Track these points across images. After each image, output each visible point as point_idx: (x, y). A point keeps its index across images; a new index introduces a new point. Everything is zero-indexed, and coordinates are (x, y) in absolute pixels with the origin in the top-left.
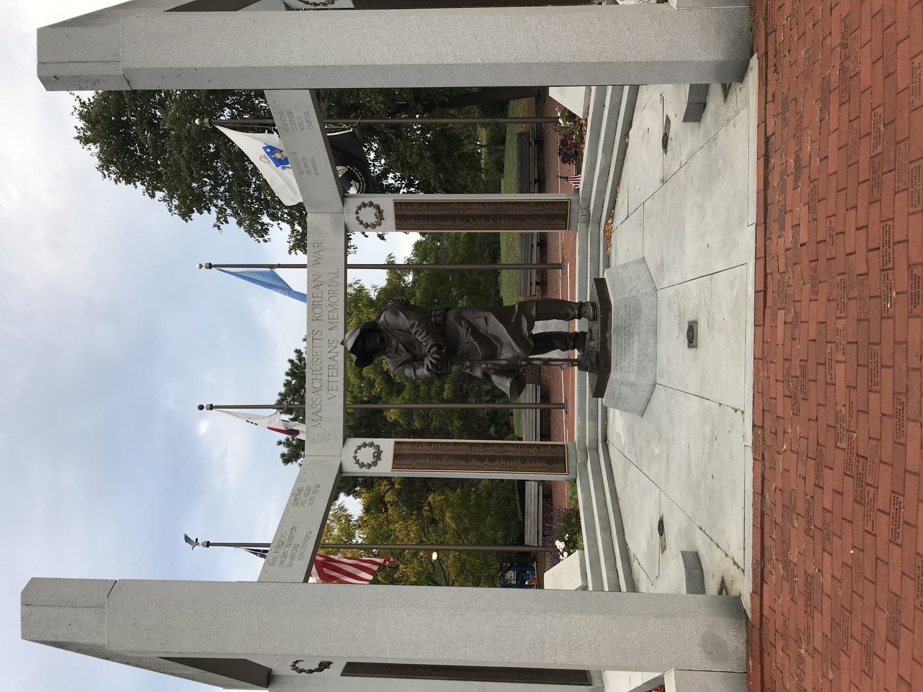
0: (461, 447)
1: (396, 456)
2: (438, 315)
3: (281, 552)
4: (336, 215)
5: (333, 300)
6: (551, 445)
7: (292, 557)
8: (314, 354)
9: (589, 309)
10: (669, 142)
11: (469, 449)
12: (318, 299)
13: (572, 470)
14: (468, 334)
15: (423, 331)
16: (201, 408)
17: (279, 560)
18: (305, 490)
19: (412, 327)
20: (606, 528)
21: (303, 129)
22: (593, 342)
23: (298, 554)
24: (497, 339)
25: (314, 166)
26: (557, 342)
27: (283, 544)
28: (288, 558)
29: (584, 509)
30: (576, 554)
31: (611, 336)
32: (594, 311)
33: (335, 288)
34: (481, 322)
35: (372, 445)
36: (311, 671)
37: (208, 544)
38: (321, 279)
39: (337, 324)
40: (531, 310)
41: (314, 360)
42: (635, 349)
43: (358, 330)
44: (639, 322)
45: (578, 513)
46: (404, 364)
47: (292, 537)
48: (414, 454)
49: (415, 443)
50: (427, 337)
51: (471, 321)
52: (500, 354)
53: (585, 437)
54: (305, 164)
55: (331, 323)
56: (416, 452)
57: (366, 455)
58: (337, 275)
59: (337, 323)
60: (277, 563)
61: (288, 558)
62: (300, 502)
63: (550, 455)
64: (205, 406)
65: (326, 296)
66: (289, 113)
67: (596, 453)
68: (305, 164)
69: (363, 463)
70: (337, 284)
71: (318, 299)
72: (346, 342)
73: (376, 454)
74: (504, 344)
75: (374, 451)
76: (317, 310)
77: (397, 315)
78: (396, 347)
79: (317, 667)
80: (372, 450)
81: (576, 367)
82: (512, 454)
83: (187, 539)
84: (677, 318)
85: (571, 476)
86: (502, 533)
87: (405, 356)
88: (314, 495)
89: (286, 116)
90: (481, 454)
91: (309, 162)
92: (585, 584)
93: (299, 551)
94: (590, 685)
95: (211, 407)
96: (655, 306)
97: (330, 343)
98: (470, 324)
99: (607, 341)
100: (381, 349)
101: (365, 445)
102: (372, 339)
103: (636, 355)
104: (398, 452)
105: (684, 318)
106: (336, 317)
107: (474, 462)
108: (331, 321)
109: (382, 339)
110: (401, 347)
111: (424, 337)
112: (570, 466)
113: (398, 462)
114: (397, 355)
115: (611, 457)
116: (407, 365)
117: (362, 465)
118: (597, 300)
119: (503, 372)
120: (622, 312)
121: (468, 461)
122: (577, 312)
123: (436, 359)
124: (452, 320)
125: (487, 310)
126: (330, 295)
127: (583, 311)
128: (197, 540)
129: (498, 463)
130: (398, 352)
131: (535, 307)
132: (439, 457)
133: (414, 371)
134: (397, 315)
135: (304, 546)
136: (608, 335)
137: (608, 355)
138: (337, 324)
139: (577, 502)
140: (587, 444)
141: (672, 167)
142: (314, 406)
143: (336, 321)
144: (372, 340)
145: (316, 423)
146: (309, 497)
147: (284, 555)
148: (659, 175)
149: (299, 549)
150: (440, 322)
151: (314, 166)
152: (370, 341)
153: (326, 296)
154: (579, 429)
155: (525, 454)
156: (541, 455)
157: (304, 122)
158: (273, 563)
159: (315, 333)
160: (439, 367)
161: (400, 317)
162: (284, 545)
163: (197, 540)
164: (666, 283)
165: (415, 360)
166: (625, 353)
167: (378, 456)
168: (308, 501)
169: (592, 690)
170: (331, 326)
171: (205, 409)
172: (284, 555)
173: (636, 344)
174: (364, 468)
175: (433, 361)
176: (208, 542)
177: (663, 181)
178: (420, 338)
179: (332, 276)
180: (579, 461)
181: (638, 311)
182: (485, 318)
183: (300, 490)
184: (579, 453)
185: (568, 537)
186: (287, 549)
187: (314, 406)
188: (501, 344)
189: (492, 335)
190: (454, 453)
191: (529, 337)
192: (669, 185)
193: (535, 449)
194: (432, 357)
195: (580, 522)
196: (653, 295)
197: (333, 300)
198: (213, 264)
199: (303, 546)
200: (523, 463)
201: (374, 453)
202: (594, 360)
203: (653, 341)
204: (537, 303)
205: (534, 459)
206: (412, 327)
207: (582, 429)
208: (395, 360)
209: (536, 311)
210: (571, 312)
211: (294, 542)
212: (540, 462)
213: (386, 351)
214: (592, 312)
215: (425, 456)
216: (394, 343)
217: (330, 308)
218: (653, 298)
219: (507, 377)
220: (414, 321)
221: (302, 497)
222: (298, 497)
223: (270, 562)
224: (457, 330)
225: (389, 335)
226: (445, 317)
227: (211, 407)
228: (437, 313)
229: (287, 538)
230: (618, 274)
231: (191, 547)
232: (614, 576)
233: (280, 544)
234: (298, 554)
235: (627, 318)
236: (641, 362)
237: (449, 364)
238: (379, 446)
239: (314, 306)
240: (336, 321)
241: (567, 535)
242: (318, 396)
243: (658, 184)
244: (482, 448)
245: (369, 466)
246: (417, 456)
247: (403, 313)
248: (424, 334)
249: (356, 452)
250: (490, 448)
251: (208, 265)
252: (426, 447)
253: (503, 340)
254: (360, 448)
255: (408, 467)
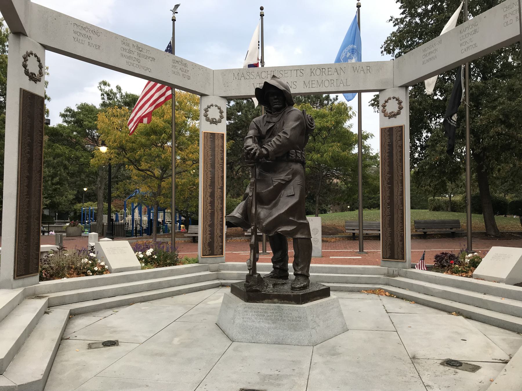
0: (220, 181)
1: (213, 135)
2: (297, 156)
3: (133, 49)
4: (392, 81)
5: (327, 83)
6: (222, 246)
7: (129, 57)
8: (286, 72)
9: (301, 284)
10: (452, 369)
11: (219, 187)
12: (327, 72)
13: (204, 260)
14: (279, 181)
15: (280, 142)
16: (262, 9)
17: (127, 47)
18: (185, 68)
19: (285, 133)
20: (151, 287)
21: (461, 45)
22: (272, 286)
23: (132, 62)
24: (275, 205)
25: (430, 59)
26: (280, 253)
27: (140, 51)
28: (129, 55)
29: (172, 270)
30: (138, 264)
31: (275, 303)
32: (299, 288)
33: (335, 84)
34: (289, 191)
35: (222, 117)
36: (25, 66)
37: (174, 20)
38: (342, 73)
39: (308, 87)
40: (302, 234)
41: (281, 72)
42: (263, 325)
43: (284, 89)
44: (286, 329)
45: (175, 264)
46: (258, 128)
47: (147, 57)
48: (214, 147)
49: (223, 148)
50: (274, 146)
51: (291, 183)
52: (263, 208)
53: (228, 270)
54: (432, 52)
55: (309, 83)
56: (216, 149)
57: (214, 113)
58: (345, 85)
59: (309, 88)
60: (124, 46)
61: (129, 55)
62: (176, 65)
63: (216, 244)
64: (263, 11)
65: (329, 78)
66: (475, 31)
67: (215, 278)
68: (432, 52)
69: (208, 111)
70: (338, 85)
71: (327, 72)
72: (274, 80)
73: (214, 120)
74: (271, 211)
75: (217, 119)
76: (318, 72)
77: (296, 120)
78: (271, 121)
79: (30, 71)
80: (217, 117)
81: (248, 272)
82: (216, 217)
83: (177, 6)
84: (277, 373)
85: (200, 260)
86: (194, 211)
87: (264, 130)
88: (181, 75)
89: (473, 29)
90: (216, 195)
91: (432, 55)
92: (113, 271)
93: (134, 62)
94: (14, 278)
95: (262, 15)
96: (299, 344)
97: (295, 83)
98: (288, 182)
99: (271, 299)
100: (271, 110)
101: (221, 112)
102: (277, 101)
103: (257, 325)
104: (216, 136)
105: (272, 384)
106: (314, 86)
107: (209, 190)
108: (311, 82)
109: (278, 110)
110: (270, 126)
111: (275, 143)
112: (207, 259)
113: (209, 136)
114: (265, 122)
115: (207, 290)
116: (257, 131)
117: (206, 110)
118: (311, 289)
119: (246, 212)
120: (295, 314)
121: (210, 186)
122: (300, 273)
123: (255, 153)
124: (292, 167)
125: (301, 196)
126: (330, 81)
127: (300, 278)
128: (177, 13)
129: (209, 207)
130: (267, 124)
131: (304, 237)
132: (213, 166)
133: (251, 137)
134: (297, 119)
135: (139, 67)
136: (276, 300)
137: (259, 300)
138: (308, 87)
139: (183, 264)
140: (222, 272)
141: (426, 373)
142: (248, 74)
143: (311, 87)
144: (276, 101)
145: (236, 76)
146: (180, 71)
147: (130, 52)
148: (421, 353)
149: (136, 62)
150: (290, 157)
151: (430, 59)
152: (275, 99)
153: (329, 78)
154: (234, 265)
155: (216, 227)
156: (215, 238)
157: (468, 45)
158: (124, 43)
159: (301, 71)
160: (248, 156)
161: (293, 122)
162: (139, 52)
163: (177, 13)
164: (317, 359)
165: (260, 139)
166: (258, 315)
167: (214, 122)
168: (176, 70)
169: (10, 280)
170: (307, 82)
171: (261, 11)
172: (130, 52)
173: (267, 325)
174: (204, 112)
175: (253, 151)
176: (175, 20)
177: (414, 358)
178: (274, 139)
179: (344, 81)
180: (211, 265)
181: (295, 328)
182: (294, 195)
183: (185, 65)
184: (217, 265)
185: (154, 257)
186: (136, 53)
187: (248, 74)
188: (271, 209)
189: (279, 200)
190: (216, 176)
191: (276, 232)
192: (408, 367)
193: (220, 234)
194: (256, 150)
195: (166, 266)
196: (310, 342)
197: (327, 83)
198: (360, 8)
199: (139, 66)
200: (209, 226)
201: (215, 119)
202: (254, 288)
203: (269, 340)
204: (307, 239)
205: (212, 233)
206: (285, 133)
207: (234, 268)
208: (262, 121)
209: (300, 238)
210: (299, 268)
211: (142, 60)
212: (211, 238)
213: (269, 114)
214: (298, 286)
215: (213, 155)
216: (275, 119)
217: (320, 82)
218: (306, 342)
219: (242, 214)
220: (289, 133)
221: (179, 66)
222: (180, 63)
223: (125, 41)
224: (284, 171)
225: (280, 115)
226: (296, 161)
227: (262, 15)
228: (299, 155)
229: (146, 54)
230: (332, 308)
231: (172, 9)
232: (111, 295)
233: (141, 49)
234: (132, 62)
235: (289, 319)
236: (251, 329)
237: (252, 164)
238: (220, 122)
239: (321, 70)
240: (311, 87)
241: (156, 257)
242: (255, 76)
243: (411, 350)
244: (220, 196)
245: (206, 116)
246: (213, 149)
247: (298, 125)
248: (278, 143)
249: (216, 106)
250: (220, 202)
251: (359, 5)
252: (220, 157)
253: (274, 210)
254: (219, 108)
255: (206, 143)
